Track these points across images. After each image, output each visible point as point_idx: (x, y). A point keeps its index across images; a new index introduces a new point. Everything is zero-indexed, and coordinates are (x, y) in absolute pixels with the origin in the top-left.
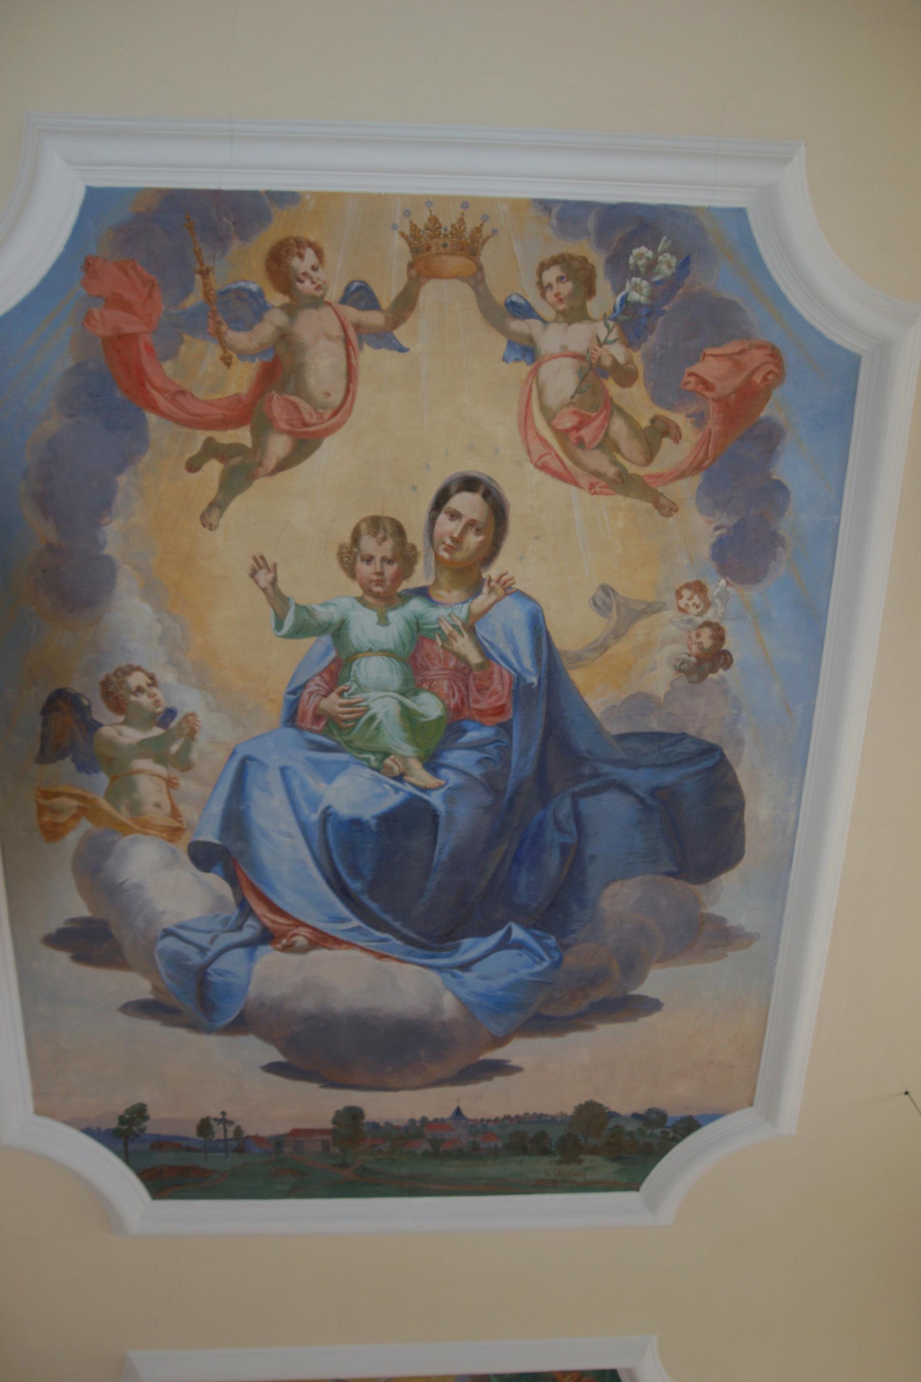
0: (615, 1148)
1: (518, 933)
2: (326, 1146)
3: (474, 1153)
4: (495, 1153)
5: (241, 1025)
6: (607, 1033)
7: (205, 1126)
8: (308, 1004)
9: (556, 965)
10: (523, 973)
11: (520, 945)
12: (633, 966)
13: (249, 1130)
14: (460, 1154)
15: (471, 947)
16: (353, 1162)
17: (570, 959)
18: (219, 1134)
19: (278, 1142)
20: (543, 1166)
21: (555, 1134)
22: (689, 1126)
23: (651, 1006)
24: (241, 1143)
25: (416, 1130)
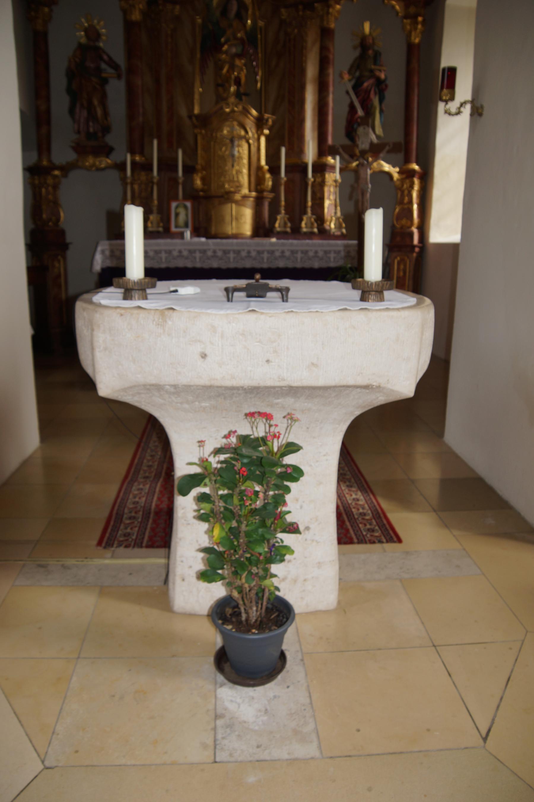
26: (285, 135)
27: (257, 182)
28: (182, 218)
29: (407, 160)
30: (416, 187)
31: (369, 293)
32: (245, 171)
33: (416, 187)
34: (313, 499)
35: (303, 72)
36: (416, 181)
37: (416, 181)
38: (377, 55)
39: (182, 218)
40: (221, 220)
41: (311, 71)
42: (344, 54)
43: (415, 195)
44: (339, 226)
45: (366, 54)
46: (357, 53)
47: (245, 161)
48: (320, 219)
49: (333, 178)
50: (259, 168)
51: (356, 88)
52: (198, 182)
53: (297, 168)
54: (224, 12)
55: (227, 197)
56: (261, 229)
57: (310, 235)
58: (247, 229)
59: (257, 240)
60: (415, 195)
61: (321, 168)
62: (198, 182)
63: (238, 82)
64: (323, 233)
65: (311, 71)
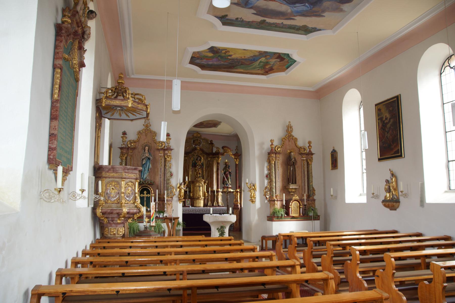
0: (306, 30)
1: (307, 4)
2: (257, 23)
3: (282, 27)
4: (285, 28)
5: (251, 8)
6: (314, 18)
7: (237, 19)
8: (265, 7)
9: (311, 9)
10: (304, 9)
11: (306, 6)
12: (323, 11)
13: (244, 20)
14: (280, 27)
15: (297, 5)
16: (261, 26)
17: (314, 9)
18: (239, 19)
19: (249, 22)
20: (293, 31)
21: (297, 27)
22: (320, 30)
23: (324, 16)
24: (243, 21)
25: (274, 24)
26: (210, 185)
27: (204, 195)
28: (188, 203)
29: (237, 189)
30: (239, 195)
31: (230, 214)
32: (202, 193)
33: (239, 195)
34: (227, 230)
35: (213, 170)
36: (239, 193)
37: (239, 193)
38: (229, 166)
39: (188, 203)
40: (196, 203)
41: (215, 170)
42: (222, 167)
43: (239, 196)
44: (222, 204)
45: (227, 166)
46: (225, 166)
47: (202, 190)
48: (218, 203)
49: (220, 194)
50: (205, 192)
51: (225, 173)
52: (191, 195)
53: (213, 192)
54: (197, 159)
55: (198, 198)
56: (205, 205)
57: (216, 206)
58: (202, 205)
59: (205, 208)
60: (239, 196)
61: (218, 192)
62: (191, 195)
63: (200, 174)
64: (219, 206)
65: (215, 170)
